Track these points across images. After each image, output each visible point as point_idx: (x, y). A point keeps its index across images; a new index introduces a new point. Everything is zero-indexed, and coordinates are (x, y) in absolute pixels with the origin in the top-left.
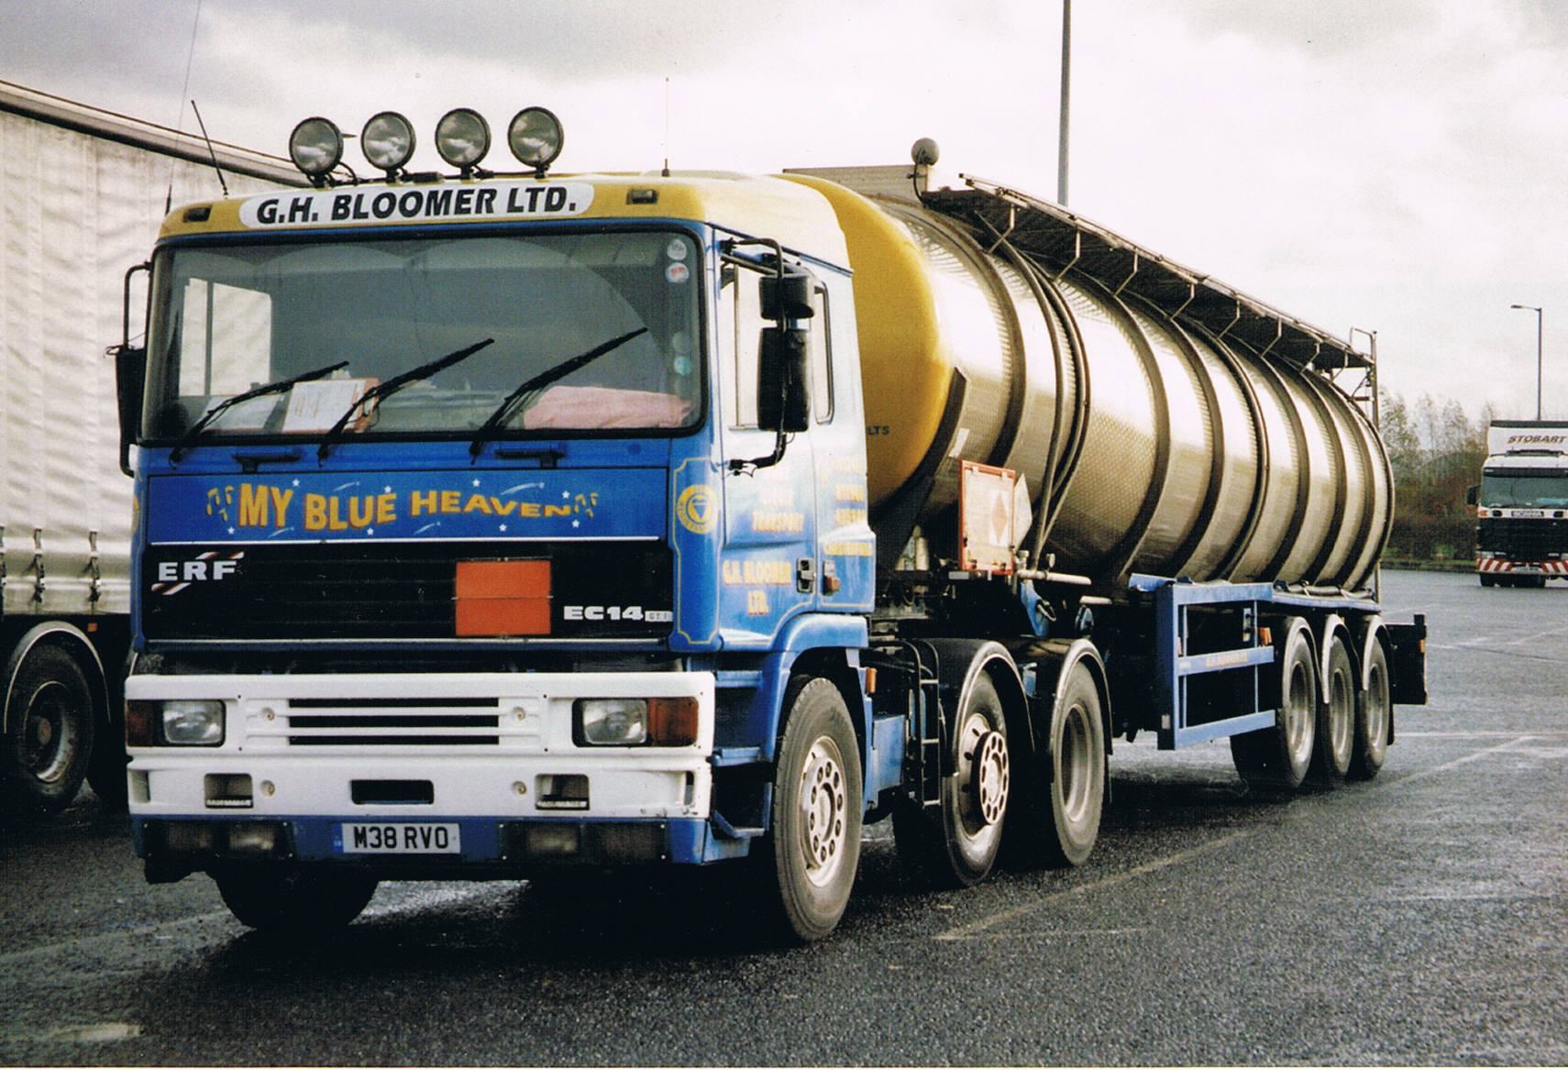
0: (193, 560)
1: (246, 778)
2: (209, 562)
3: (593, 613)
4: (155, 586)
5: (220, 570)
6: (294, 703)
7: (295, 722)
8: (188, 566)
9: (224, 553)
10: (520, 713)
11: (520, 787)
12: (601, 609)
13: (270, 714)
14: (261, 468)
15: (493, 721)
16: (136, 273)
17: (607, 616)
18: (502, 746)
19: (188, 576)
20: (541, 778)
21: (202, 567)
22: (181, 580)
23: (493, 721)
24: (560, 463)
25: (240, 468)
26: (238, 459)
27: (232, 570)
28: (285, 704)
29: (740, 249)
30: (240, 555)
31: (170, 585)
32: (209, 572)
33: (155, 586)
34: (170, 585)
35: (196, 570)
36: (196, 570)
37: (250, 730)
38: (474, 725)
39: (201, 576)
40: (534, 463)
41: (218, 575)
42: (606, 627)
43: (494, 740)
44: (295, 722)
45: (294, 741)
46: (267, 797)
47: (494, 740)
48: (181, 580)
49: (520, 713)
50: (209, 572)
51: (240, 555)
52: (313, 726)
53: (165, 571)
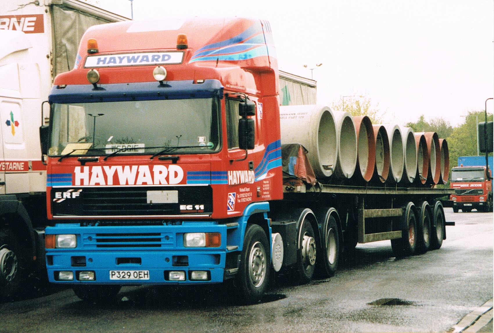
0: (66, 191)
1: (84, 257)
2: (71, 193)
3: (189, 207)
4: (54, 200)
5: (75, 195)
6: (98, 235)
7: (98, 240)
8: (65, 193)
9: (76, 189)
10: (167, 238)
11: (167, 260)
12: (192, 206)
13: (90, 238)
15: (159, 240)
16: (45, 103)
17: (194, 208)
18: (162, 248)
19: (65, 197)
20: (174, 257)
21: (69, 194)
22: (62, 198)
23: (159, 240)
24: (178, 162)
25: (79, 163)
26: (79, 160)
27: (78, 195)
28: (95, 235)
29: (231, 96)
30: (81, 191)
31: (59, 199)
32: (71, 196)
33: (54, 200)
34: (59, 199)
35: (67, 195)
36: (67, 195)
37: (86, 243)
38: (153, 241)
39: (69, 197)
41: (74, 197)
42: (194, 211)
43: (160, 245)
44: (98, 240)
45: (98, 246)
46: (90, 263)
47: (160, 245)
48: (62, 198)
49: (167, 238)
50: (71, 196)
51: (81, 191)
52: (105, 242)
53: (58, 195)
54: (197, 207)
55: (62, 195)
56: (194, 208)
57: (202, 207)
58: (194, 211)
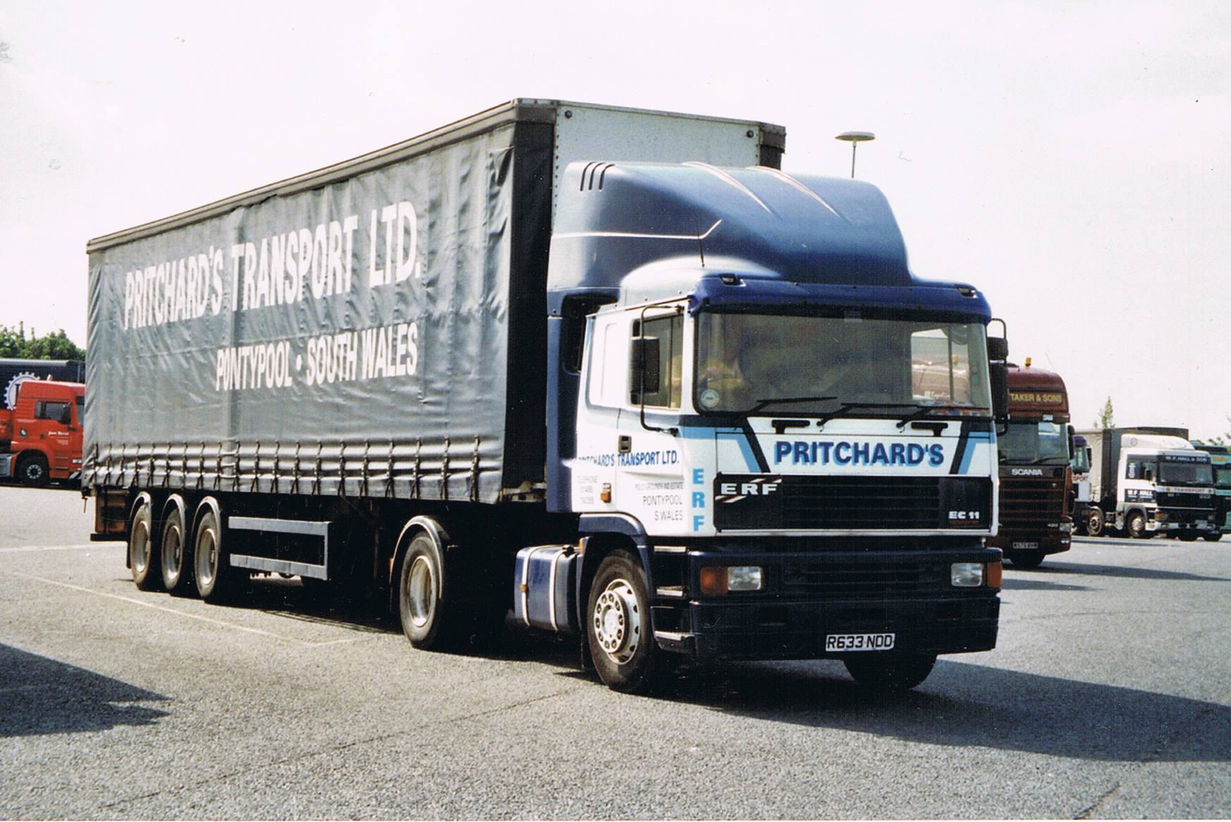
2: (760, 486)
3: (961, 515)
4: (718, 498)
5: (766, 489)
8: (745, 488)
14: (787, 430)
17: (967, 515)
19: (744, 491)
21: (755, 487)
24: (944, 432)
25: (774, 430)
26: (774, 424)
30: (779, 481)
31: (732, 496)
32: (760, 489)
33: (718, 498)
39: (754, 492)
40: (931, 433)
48: (739, 493)
50: (760, 489)
51: (779, 481)
53: (725, 489)
54: (971, 514)
55: (739, 490)
56: (967, 515)
57: (977, 514)
58: (967, 523)
